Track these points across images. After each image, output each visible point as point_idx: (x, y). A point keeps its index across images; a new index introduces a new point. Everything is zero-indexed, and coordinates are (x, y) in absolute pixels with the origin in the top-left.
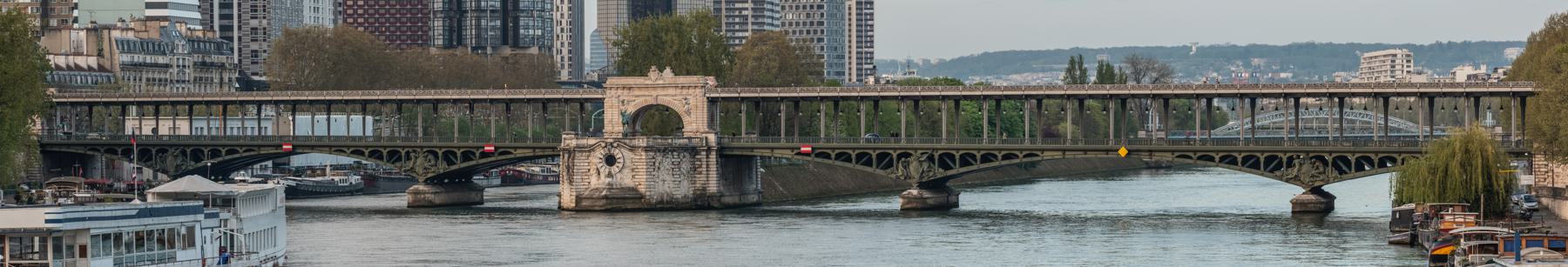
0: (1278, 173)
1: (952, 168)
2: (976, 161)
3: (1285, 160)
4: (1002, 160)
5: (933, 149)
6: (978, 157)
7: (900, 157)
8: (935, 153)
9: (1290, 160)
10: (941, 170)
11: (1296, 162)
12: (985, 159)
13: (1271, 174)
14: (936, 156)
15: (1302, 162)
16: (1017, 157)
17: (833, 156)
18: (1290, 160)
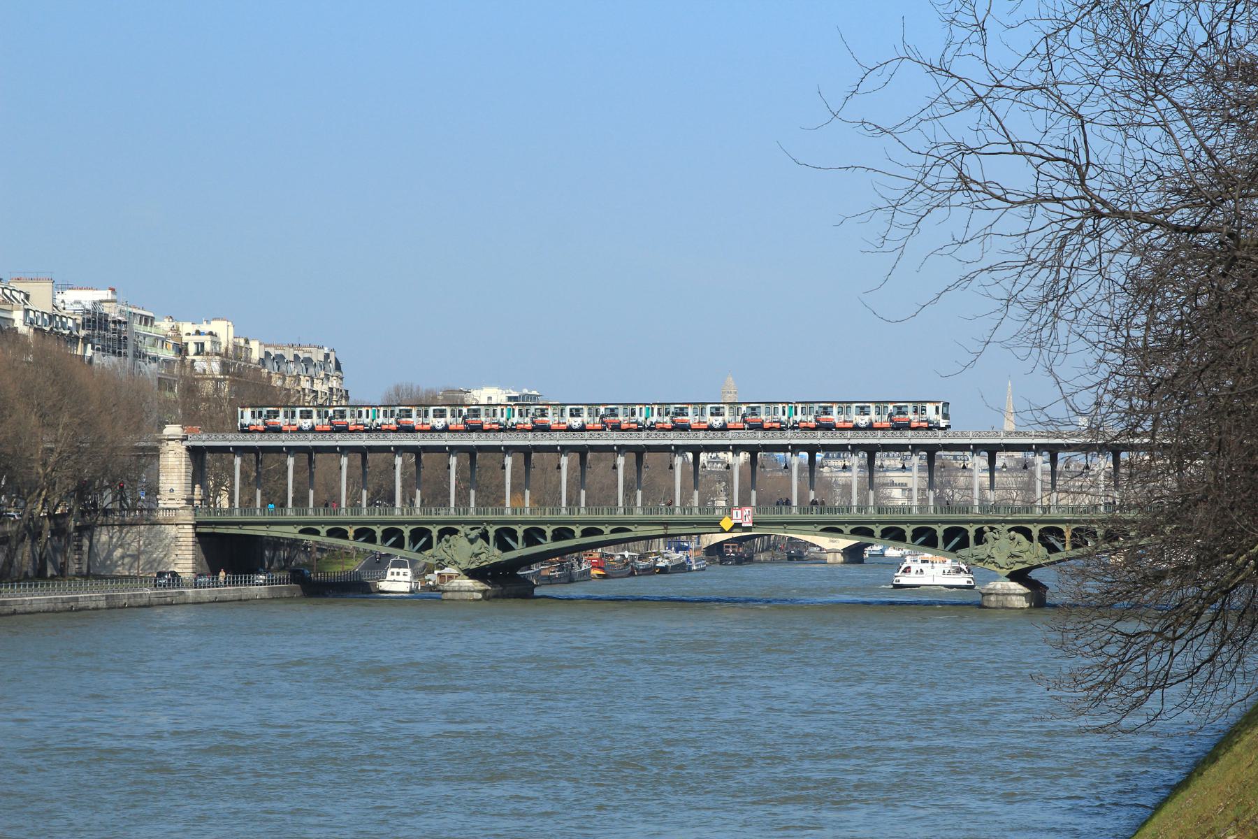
0: (962, 552)
1: (511, 549)
2: (545, 539)
3: (971, 530)
4: (582, 536)
5: (489, 523)
6: (549, 534)
7: (442, 533)
8: (488, 528)
9: (980, 533)
10: (497, 552)
11: (989, 535)
12: (560, 535)
13: (954, 554)
14: (491, 534)
15: (997, 536)
16: (601, 532)
17: (351, 533)
18: (980, 533)
